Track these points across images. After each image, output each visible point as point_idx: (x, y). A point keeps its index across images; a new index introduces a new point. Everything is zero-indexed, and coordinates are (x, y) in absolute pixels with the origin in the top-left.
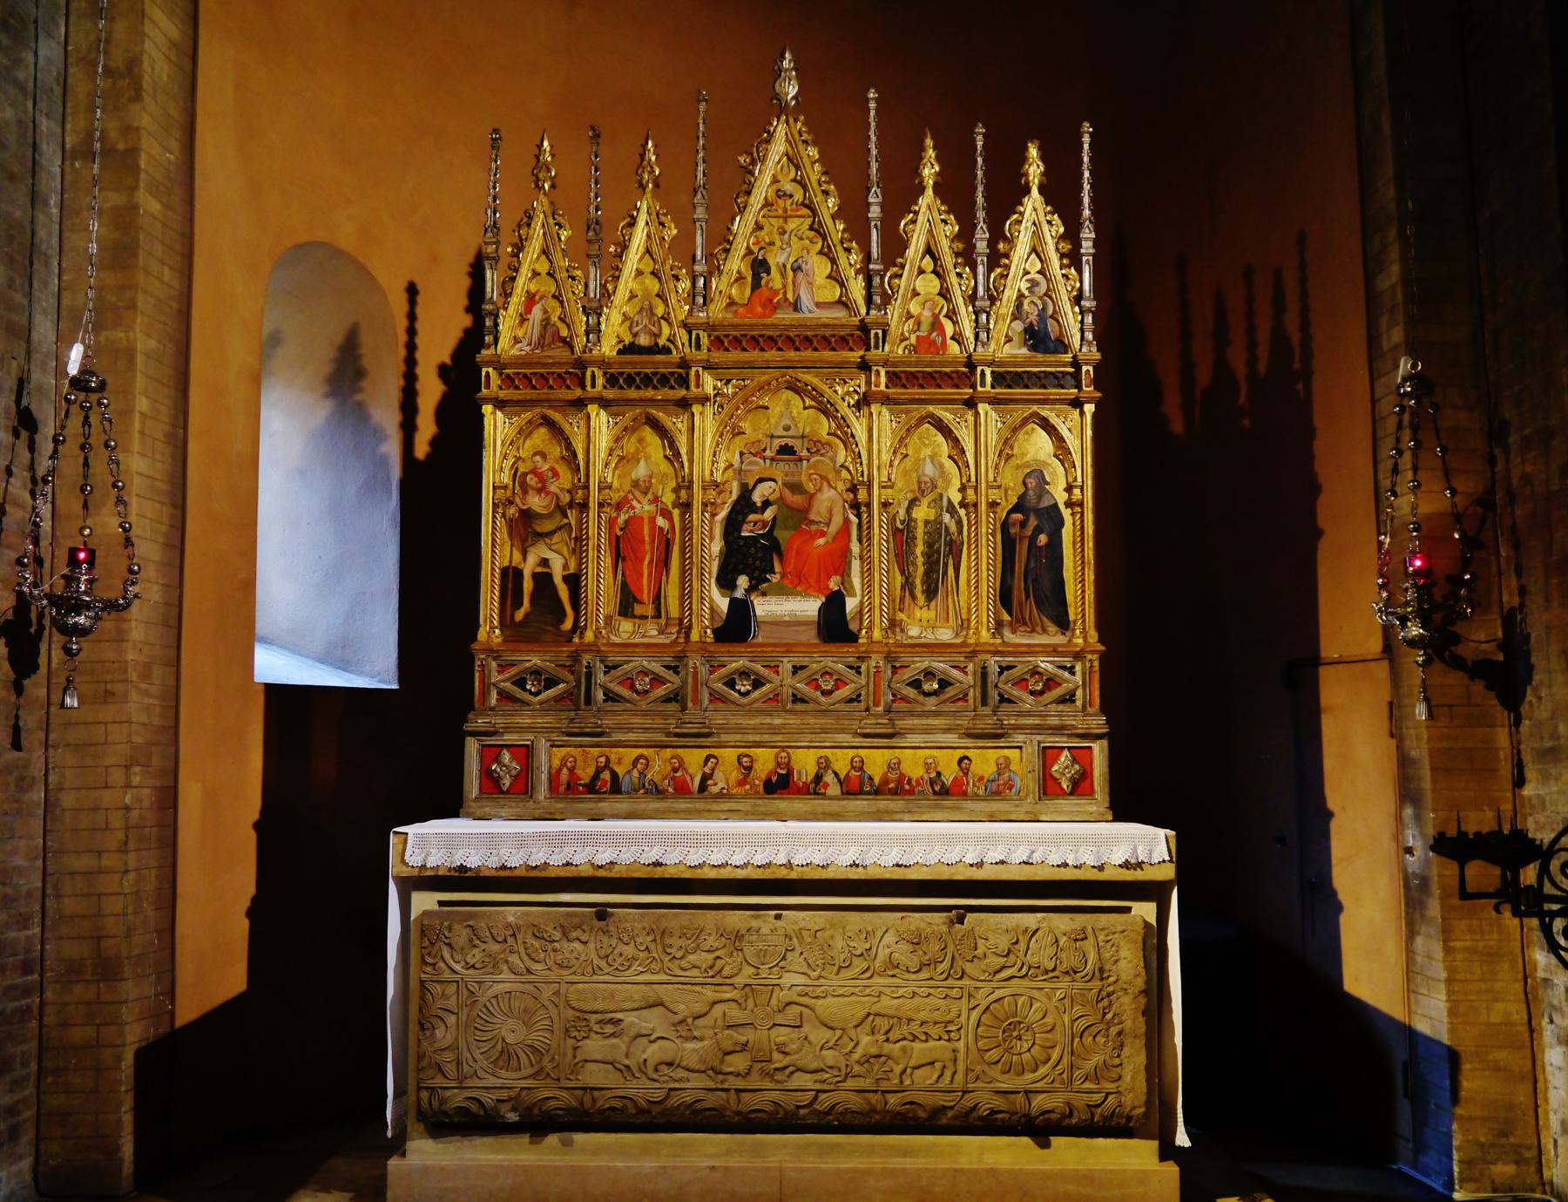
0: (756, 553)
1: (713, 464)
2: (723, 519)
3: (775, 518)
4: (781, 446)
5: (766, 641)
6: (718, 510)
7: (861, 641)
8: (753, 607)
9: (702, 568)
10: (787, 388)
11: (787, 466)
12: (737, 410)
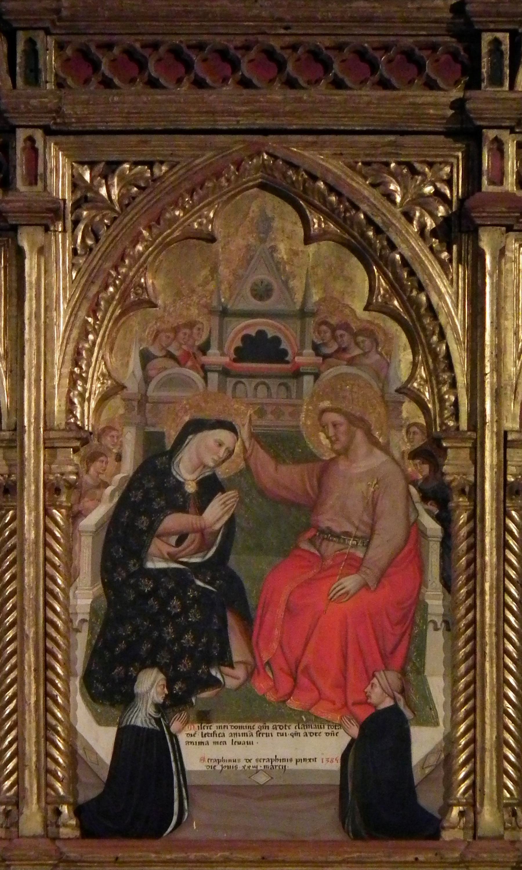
0: (185, 610)
2: (99, 526)
3: (231, 523)
4: (246, 338)
6: (86, 503)
9: (47, 650)
11: (262, 391)
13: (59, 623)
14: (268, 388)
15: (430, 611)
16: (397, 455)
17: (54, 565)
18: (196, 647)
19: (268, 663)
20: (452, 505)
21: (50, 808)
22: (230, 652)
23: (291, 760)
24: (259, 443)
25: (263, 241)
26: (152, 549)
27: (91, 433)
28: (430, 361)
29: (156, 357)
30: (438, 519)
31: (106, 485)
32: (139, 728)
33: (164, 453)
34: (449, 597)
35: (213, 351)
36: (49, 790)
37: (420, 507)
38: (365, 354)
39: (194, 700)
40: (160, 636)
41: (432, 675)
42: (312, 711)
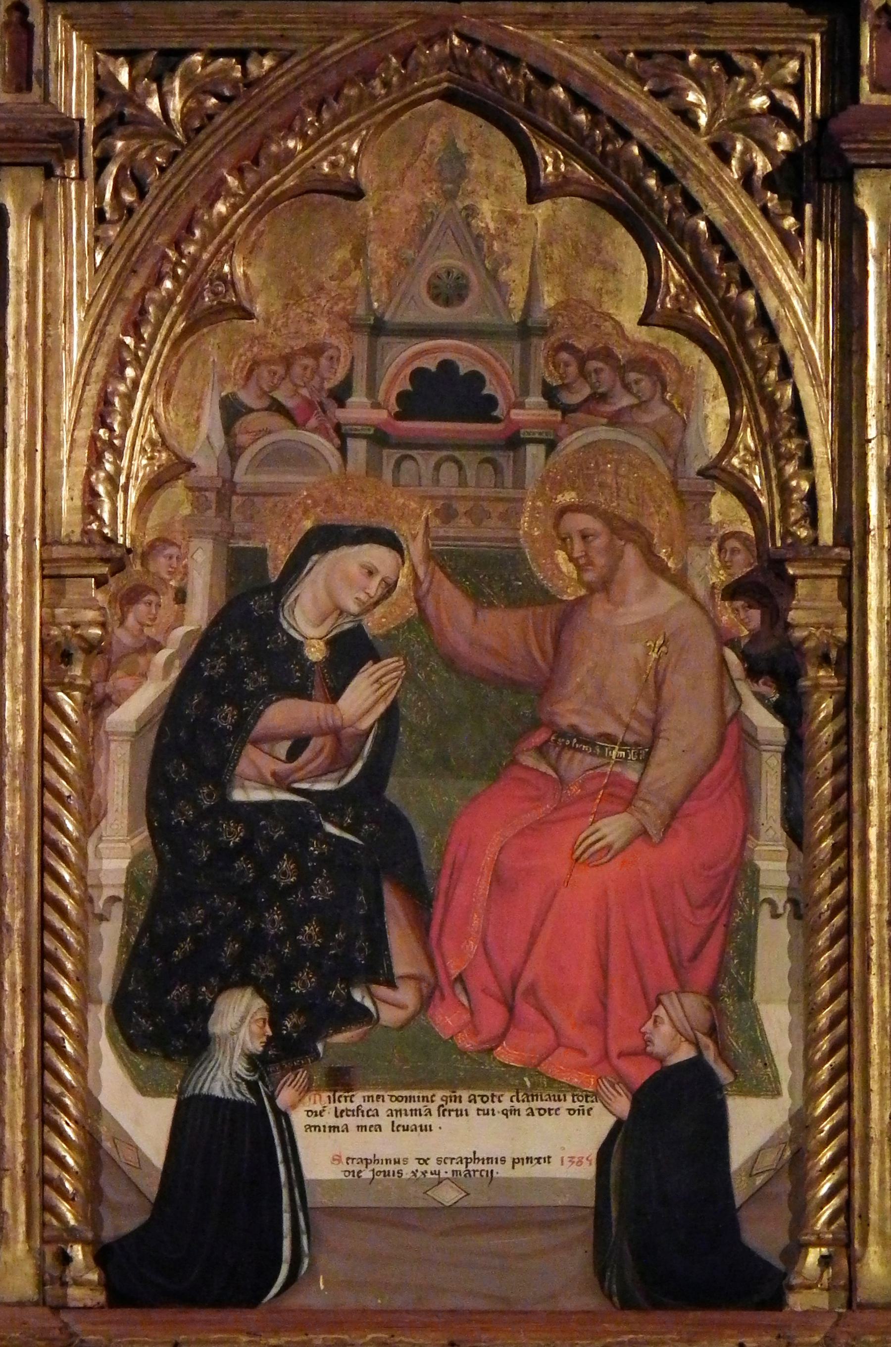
0: (304, 880)
1: (96, 460)
2: (143, 724)
4: (418, 375)
5: (349, 1300)
6: (120, 680)
7: (797, 1301)
8: (290, 1143)
9: (45, 955)
10: (450, 97)
11: (449, 472)
12: (211, 201)
13: (69, 903)
14: (461, 468)
15: (762, 881)
16: (701, 592)
17: (58, 796)
18: (324, 948)
19: (460, 979)
20: (805, 683)
21: (49, 1250)
22: (389, 957)
23: (503, 1160)
24: (442, 568)
25: (451, 196)
26: (243, 766)
27: (129, 551)
28: (763, 417)
29: (251, 410)
30: (777, 709)
31: (157, 647)
32: (218, 1099)
33: (267, 588)
34: (799, 856)
35: (358, 398)
36: (48, 1217)
37: (745, 689)
38: (642, 405)
39: (320, 1047)
40: (257, 930)
41: (768, 1002)
42: (543, 1068)
